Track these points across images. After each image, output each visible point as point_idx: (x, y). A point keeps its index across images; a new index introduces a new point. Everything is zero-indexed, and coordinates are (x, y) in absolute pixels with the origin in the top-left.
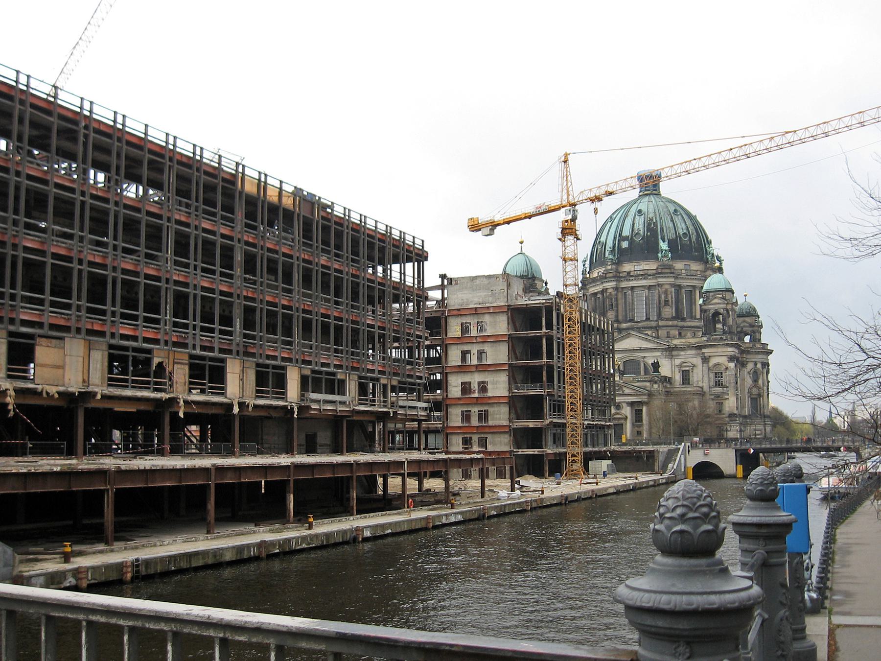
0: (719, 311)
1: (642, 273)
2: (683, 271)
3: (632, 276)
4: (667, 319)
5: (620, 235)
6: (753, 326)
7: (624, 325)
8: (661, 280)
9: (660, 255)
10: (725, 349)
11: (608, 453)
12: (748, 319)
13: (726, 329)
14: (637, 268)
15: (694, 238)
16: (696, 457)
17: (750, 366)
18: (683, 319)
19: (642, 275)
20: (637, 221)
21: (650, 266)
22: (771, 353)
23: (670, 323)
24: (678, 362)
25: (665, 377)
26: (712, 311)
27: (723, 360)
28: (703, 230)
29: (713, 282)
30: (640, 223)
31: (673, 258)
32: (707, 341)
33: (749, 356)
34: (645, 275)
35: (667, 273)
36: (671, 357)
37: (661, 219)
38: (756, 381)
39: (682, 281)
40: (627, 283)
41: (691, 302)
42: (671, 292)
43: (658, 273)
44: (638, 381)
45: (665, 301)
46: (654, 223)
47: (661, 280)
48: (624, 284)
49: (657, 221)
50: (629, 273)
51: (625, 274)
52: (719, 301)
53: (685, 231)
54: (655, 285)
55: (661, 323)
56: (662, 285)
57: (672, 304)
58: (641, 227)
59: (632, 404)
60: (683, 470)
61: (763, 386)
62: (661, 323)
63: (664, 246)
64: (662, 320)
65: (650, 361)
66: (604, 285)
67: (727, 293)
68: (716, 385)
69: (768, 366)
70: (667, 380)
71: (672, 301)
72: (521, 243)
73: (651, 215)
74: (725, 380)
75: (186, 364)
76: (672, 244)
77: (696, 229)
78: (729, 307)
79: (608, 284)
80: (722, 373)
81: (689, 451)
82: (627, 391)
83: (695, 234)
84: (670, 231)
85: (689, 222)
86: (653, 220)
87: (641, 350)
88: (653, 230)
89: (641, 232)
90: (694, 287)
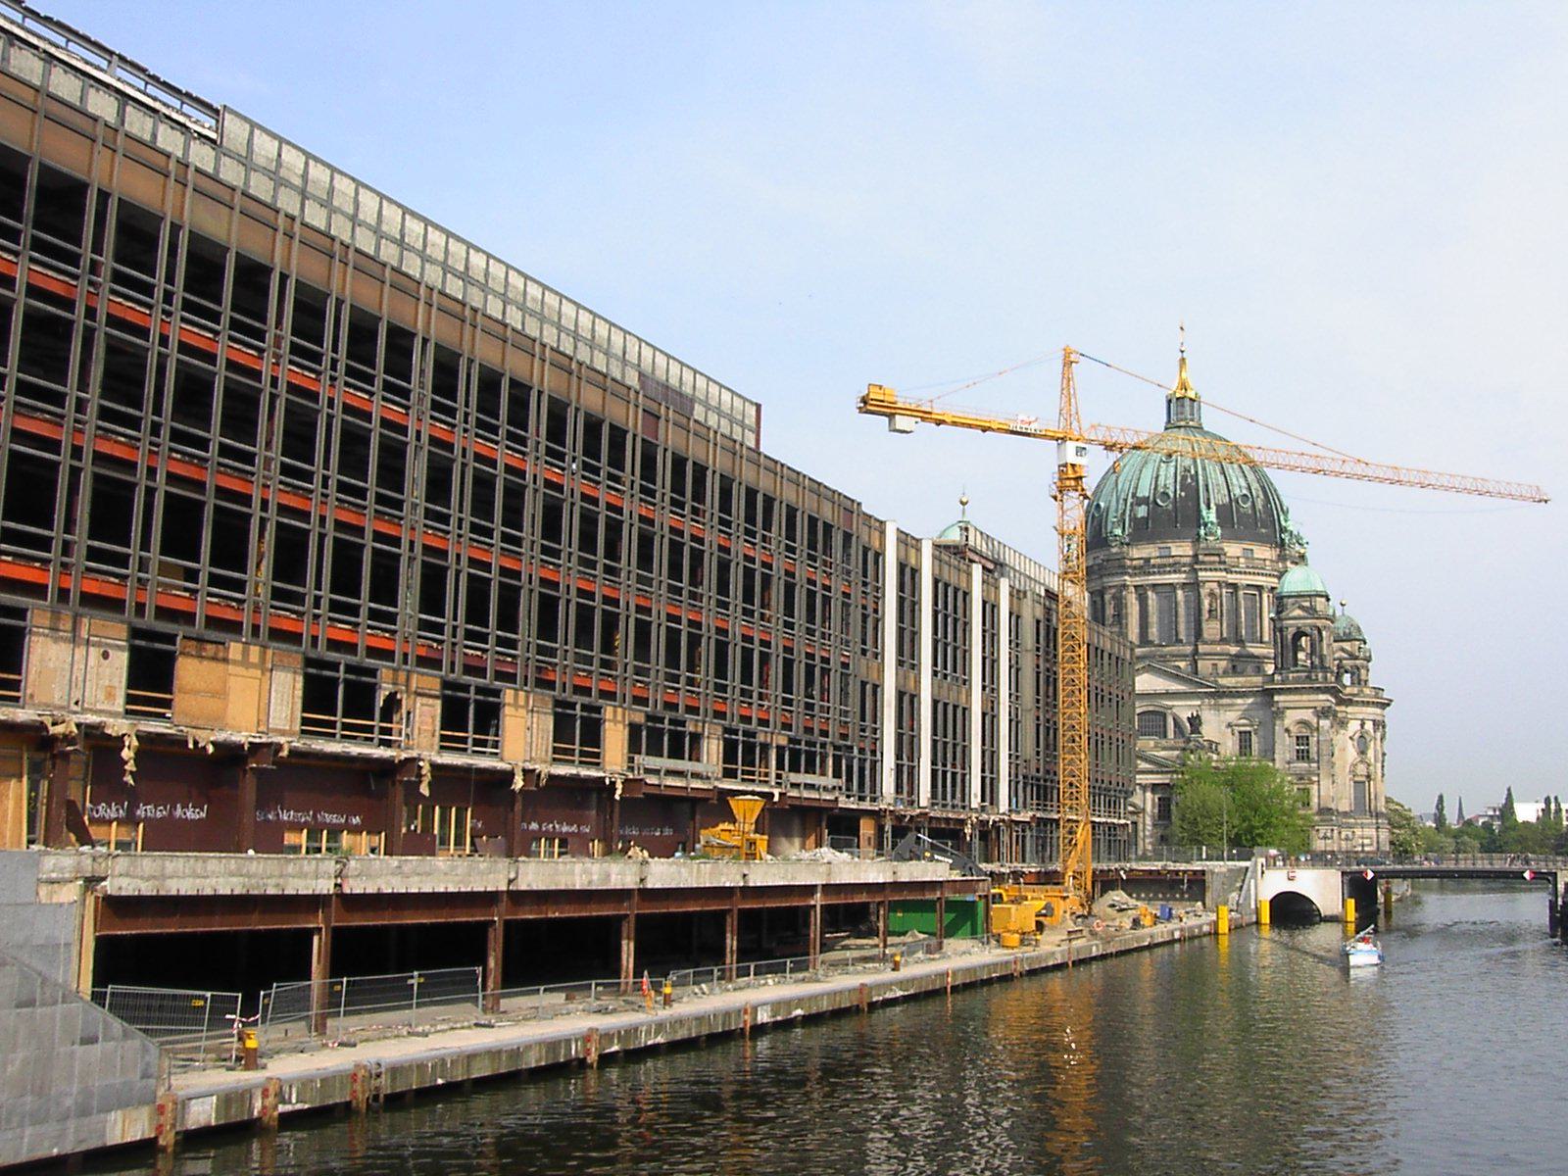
0: (1303, 629)
1: (1171, 560)
2: (1242, 560)
3: (1154, 566)
4: (1213, 643)
5: (1134, 495)
9: (1202, 532)
10: (1313, 697)
11: (1122, 873)
12: (1347, 646)
13: (1317, 661)
15: (1259, 505)
16: (1272, 882)
17: (1354, 726)
19: (1170, 565)
20: (1162, 473)
21: (1182, 549)
22: (1388, 705)
23: (1219, 648)
24: (1232, 716)
25: (1211, 742)
26: (1292, 631)
27: (1308, 715)
28: (1275, 490)
29: (1296, 580)
30: (1168, 477)
31: (1225, 538)
32: (1283, 682)
33: (1350, 709)
35: (1214, 562)
36: (1217, 707)
37: (1204, 469)
38: (1363, 752)
39: (1234, 576)
41: (1255, 614)
44: (1164, 749)
45: (1210, 611)
46: (1192, 476)
49: (1196, 472)
52: (1306, 614)
53: (1245, 492)
57: (1222, 616)
59: (1154, 787)
60: (1253, 906)
61: (1376, 761)
63: (1211, 516)
64: (1206, 643)
65: (1184, 715)
67: (1318, 599)
68: (1298, 757)
69: (1384, 727)
70: (1213, 747)
73: (1188, 462)
74: (1313, 749)
75: (436, 697)
76: (1225, 514)
77: (1263, 488)
78: (1319, 623)
80: (1307, 738)
81: (1263, 873)
83: (1262, 496)
84: (1219, 491)
85: (1251, 477)
86: (1189, 471)
87: (1168, 695)
88: (1191, 490)
90: (1259, 588)
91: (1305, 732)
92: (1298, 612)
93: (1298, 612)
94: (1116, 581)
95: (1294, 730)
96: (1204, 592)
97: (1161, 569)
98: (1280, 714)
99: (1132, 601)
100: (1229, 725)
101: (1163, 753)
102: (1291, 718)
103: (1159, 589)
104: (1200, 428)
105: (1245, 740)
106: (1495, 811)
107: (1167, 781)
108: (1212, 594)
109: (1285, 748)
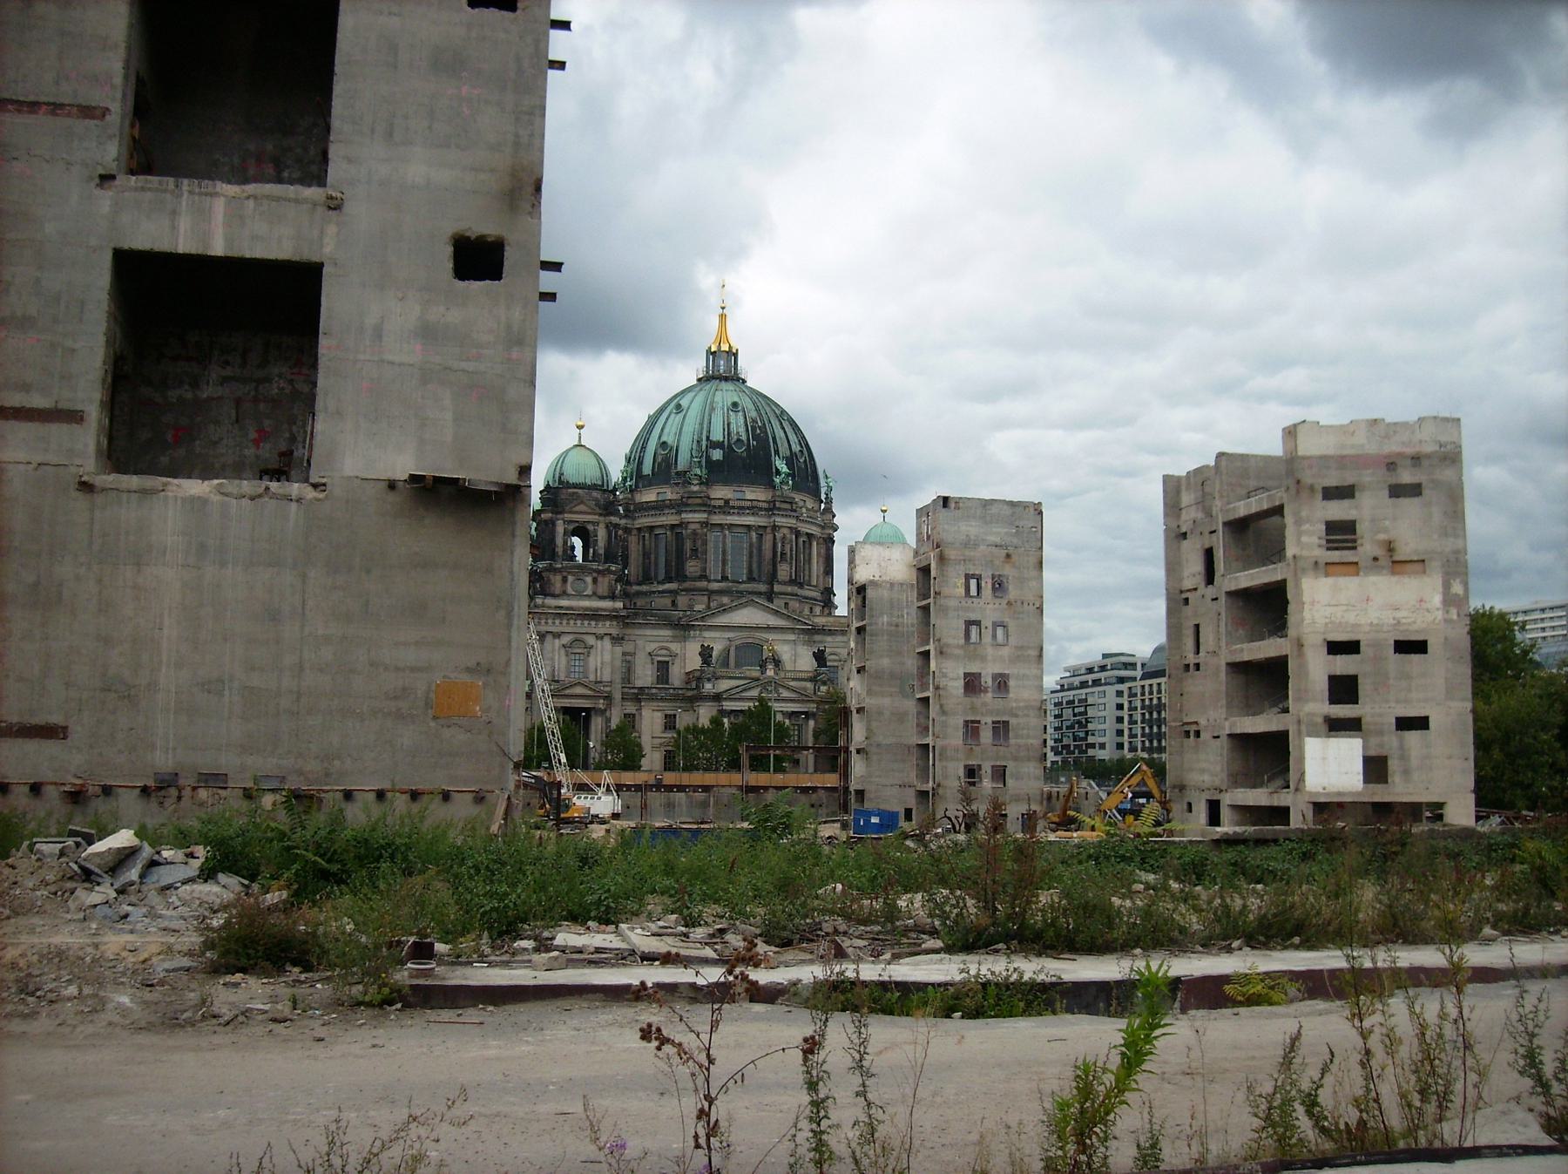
3: (733, 507)
4: (785, 583)
7: (715, 586)
8: (780, 521)
14: (739, 495)
18: (801, 585)
19: (748, 508)
34: (753, 509)
35: (786, 510)
40: (722, 517)
42: (791, 541)
43: (771, 508)
47: (780, 521)
48: (717, 519)
50: (727, 502)
51: (721, 503)
54: (766, 527)
55: (777, 588)
56: (780, 527)
57: (791, 559)
58: (742, 430)
66: (683, 516)
71: (791, 555)
72: (580, 427)
79: (690, 515)
82: (785, 694)
87: (769, 628)
89: (744, 438)
90: (809, 536)
107: (806, 710)
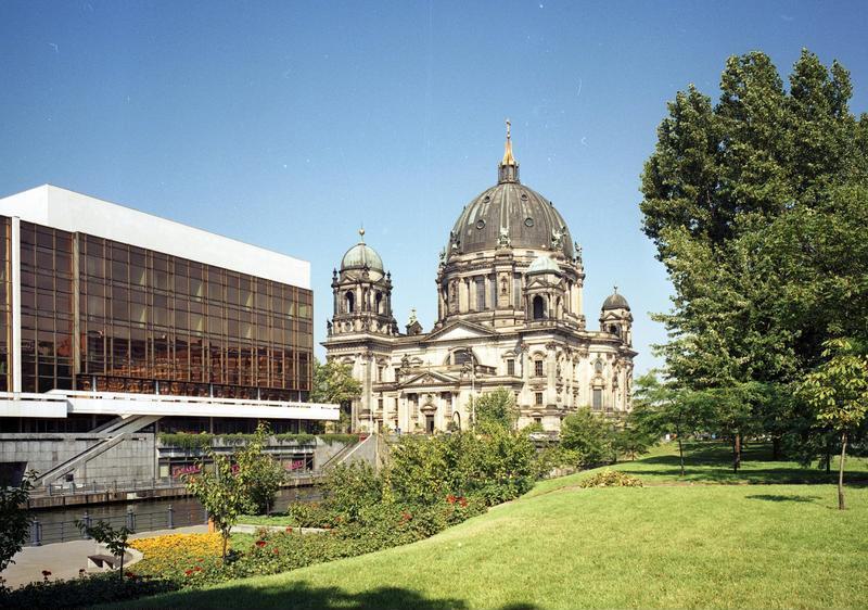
6: (619, 319)
12: (618, 312)
17: (593, 356)
23: (507, 312)
27: (542, 348)
45: (504, 290)
47: (498, 268)
55: (497, 313)
61: (609, 376)
62: (497, 313)
64: (499, 309)
78: (550, 290)
82: (436, 381)
87: (468, 339)
91: (540, 358)
92: (537, 284)
93: (537, 284)
94: (452, 276)
95: (535, 358)
96: (499, 278)
97: (476, 267)
98: (525, 348)
99: (462, 286)
100: (503, 357)
101: (451, 374)
102: (533, 349)
103: (477, 279)
104: (516, 183)
105: (511, 362)
106: (685, 404)
108: (504, 280)
109: (530, 367)
